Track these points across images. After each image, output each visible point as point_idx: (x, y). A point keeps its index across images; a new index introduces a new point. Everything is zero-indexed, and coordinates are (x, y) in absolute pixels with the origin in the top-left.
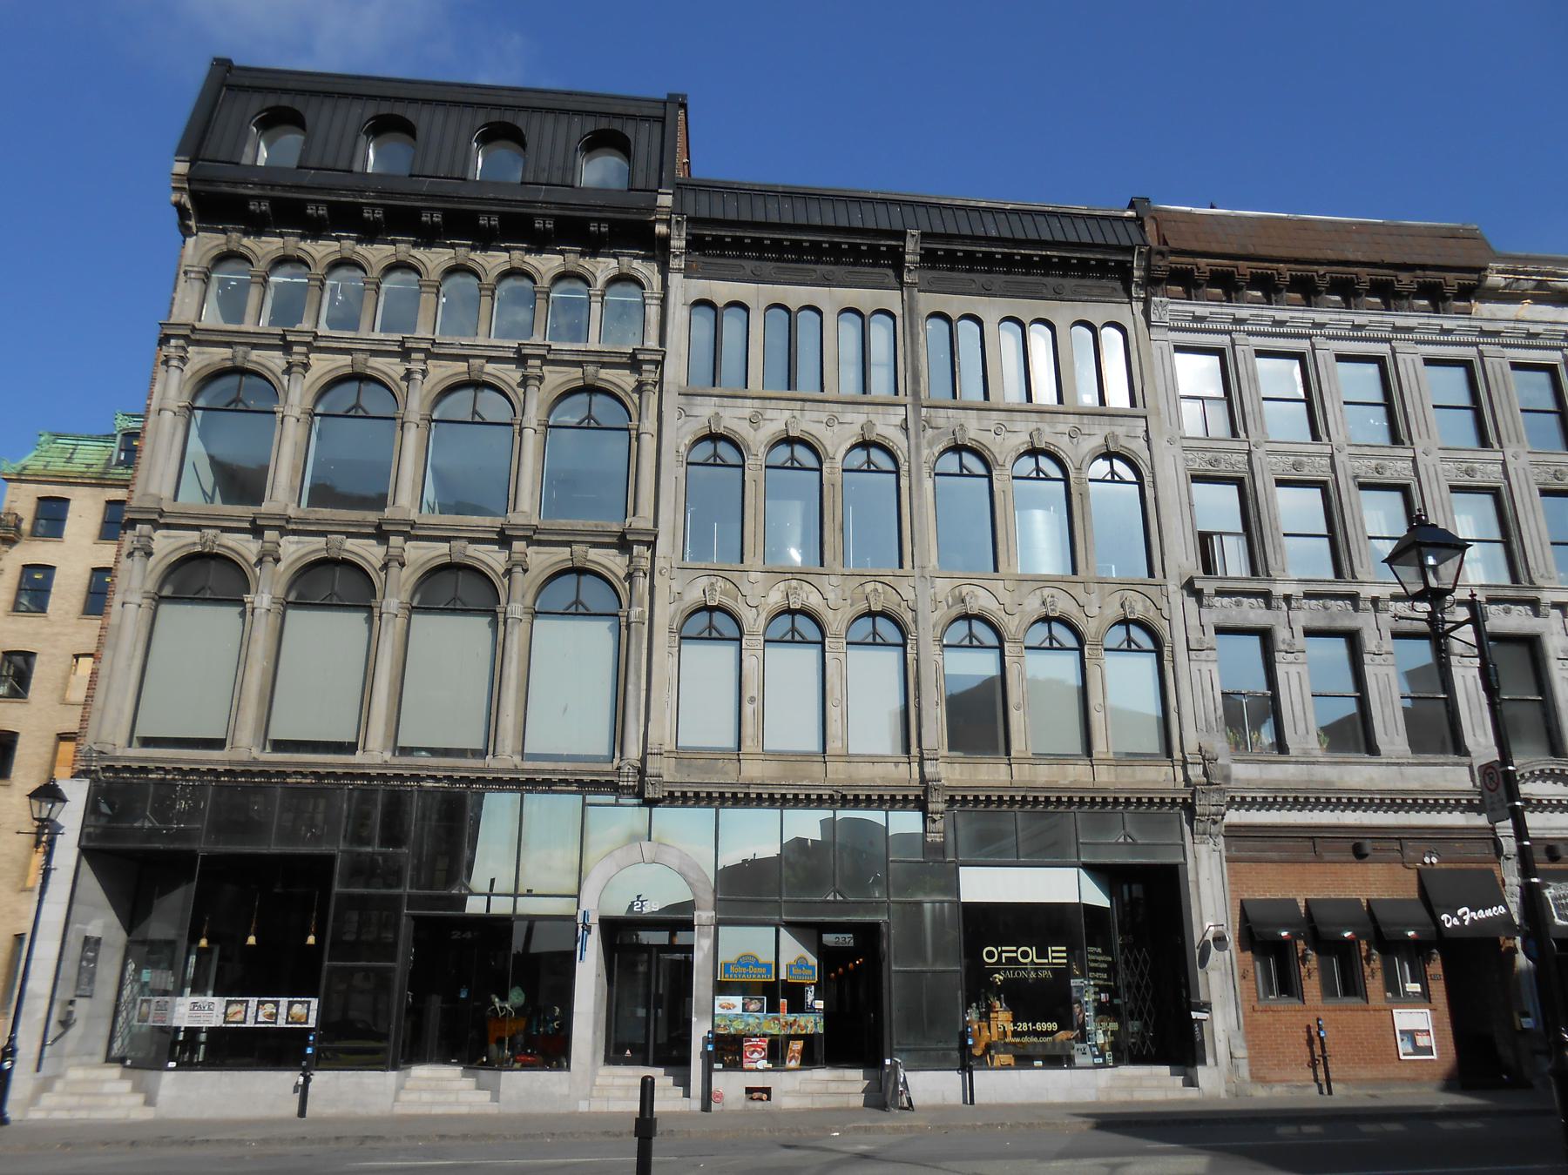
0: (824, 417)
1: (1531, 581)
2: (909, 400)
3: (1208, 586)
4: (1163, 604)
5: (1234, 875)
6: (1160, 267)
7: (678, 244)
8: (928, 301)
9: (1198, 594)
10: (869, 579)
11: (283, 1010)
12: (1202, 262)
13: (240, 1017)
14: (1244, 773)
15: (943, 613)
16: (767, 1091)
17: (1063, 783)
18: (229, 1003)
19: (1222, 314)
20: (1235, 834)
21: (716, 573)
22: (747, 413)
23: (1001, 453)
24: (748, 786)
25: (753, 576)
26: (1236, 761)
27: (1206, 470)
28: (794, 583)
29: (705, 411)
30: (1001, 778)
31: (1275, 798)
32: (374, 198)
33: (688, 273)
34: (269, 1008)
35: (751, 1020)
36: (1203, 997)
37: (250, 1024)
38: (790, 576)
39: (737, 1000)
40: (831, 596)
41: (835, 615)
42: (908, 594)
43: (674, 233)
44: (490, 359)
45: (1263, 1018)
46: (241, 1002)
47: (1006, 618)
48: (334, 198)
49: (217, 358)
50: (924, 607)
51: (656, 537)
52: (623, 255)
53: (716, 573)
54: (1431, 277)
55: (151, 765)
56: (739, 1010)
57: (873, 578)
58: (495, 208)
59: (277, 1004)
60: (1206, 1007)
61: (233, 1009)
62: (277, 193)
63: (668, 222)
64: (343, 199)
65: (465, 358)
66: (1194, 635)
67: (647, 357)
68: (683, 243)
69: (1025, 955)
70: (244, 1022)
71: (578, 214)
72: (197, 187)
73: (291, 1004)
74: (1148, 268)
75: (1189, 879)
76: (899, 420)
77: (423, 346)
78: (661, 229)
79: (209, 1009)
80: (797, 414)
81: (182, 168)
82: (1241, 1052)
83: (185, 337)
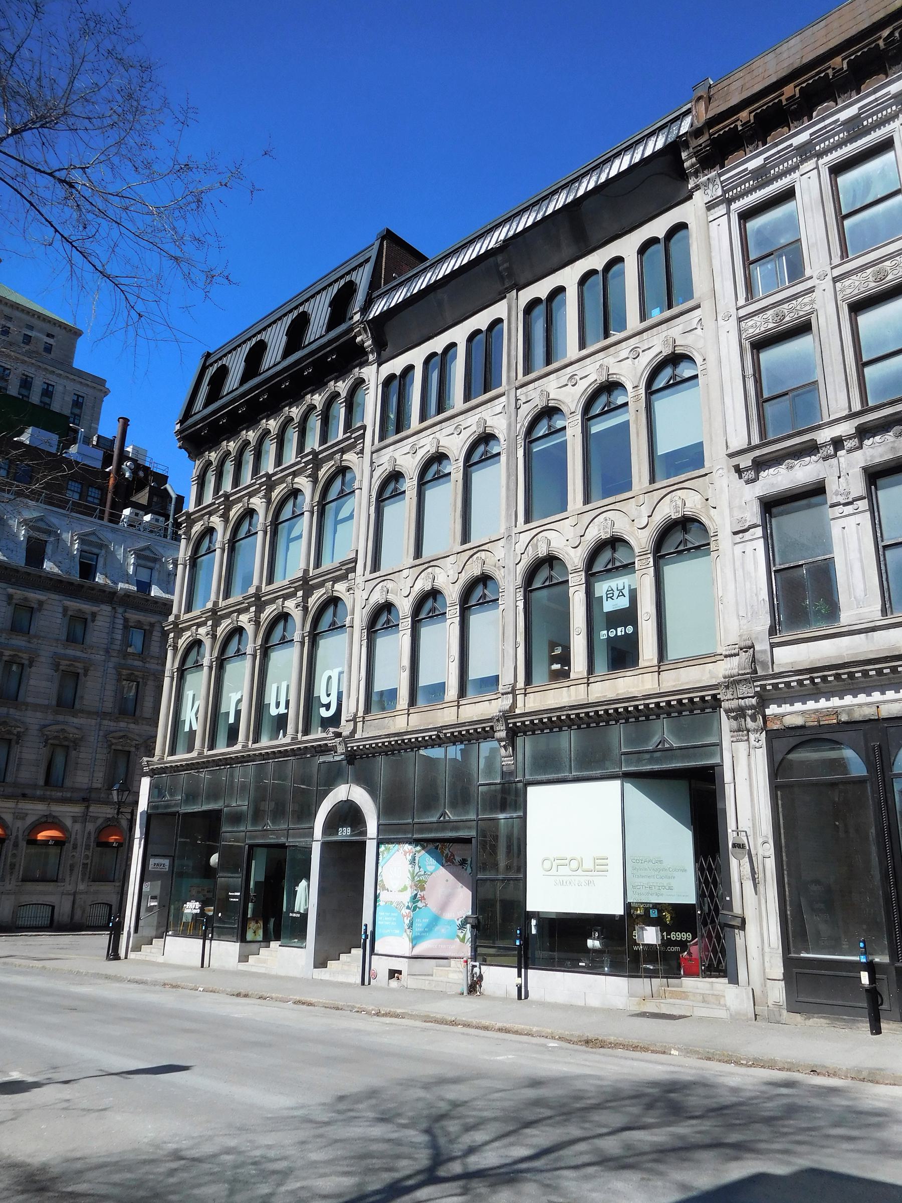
6: (700, 145)
10: (475, 550)
15: (526, 561)
16: (400, 972)
17: (611, 695)
19: (779, 152)
21: (386, 578)
22: (407, 449)
23: (573, 401)
24: (388, 736)
25: (405, 573)
27: (766, 331)
28: (430, 570)
30: (563, 700)
31: (812, 679)
36: (737, 910)
38: (426, 565)
40: (451, 572)
41: (454, 588)
47: (572, 552)
51: (356, 564)
53: (386, 578)
57: (478, 549)
75: (726, 780)
81: (178, 427)
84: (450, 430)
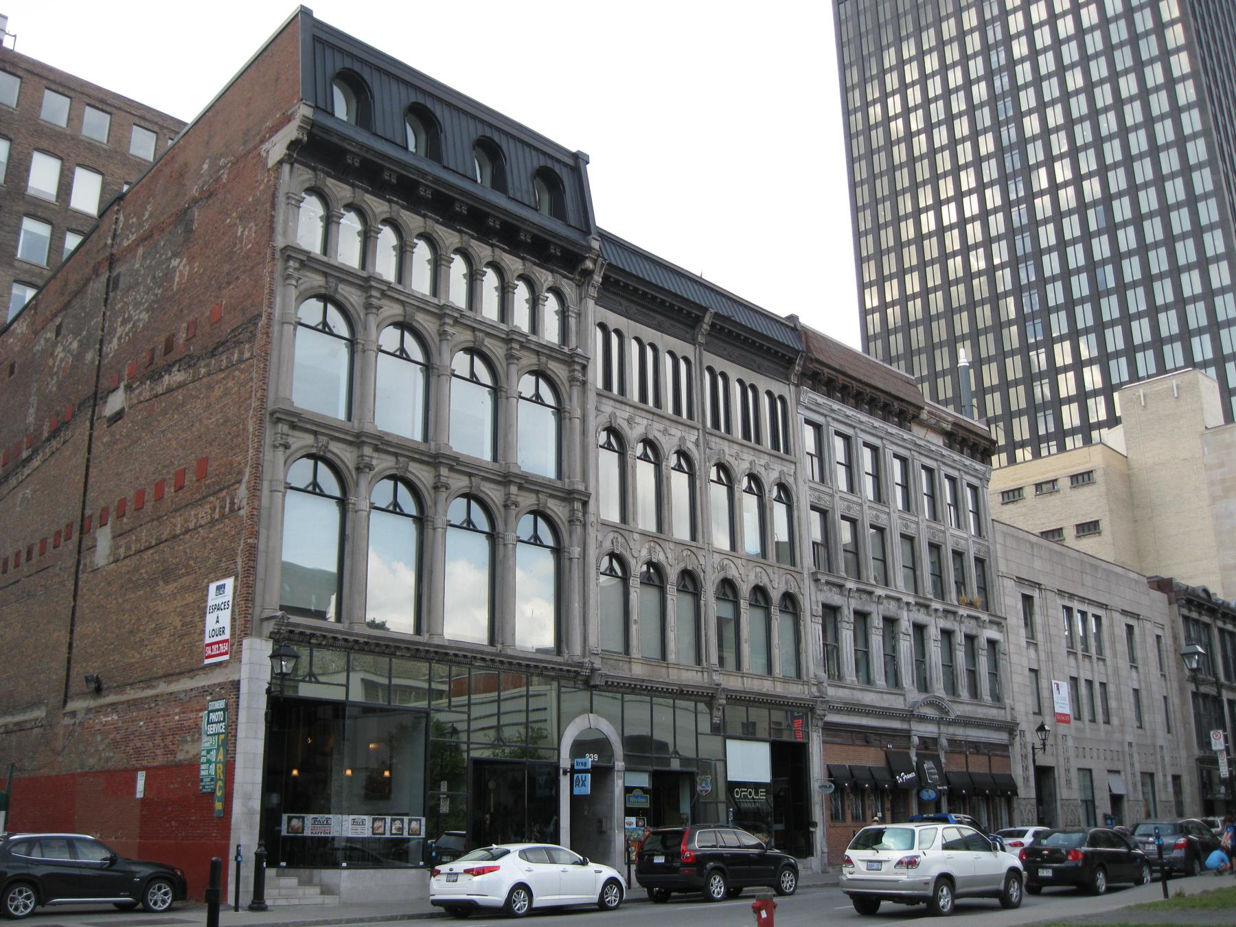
0: (661, 427)
1: (896, 587)
2: (700, 426)
3: (823, 579)
4: (801, 586)
5: (825, 750)
7: (598, 279)
8: (710, 359)
9: (817, 581)
11: (406, 825)
12: (826, 370)
13: (381, 830)
14: (831, 692)
17: (764, 690)
18: (374, 820)
20: (830, 728)
22: (626, 415)
26: (829, 685)
29: (608, 407)
32: (430, 181)
33: (598, 302)
34: (398, 824)
35: (640, 832)
37: (388, 835)
39: (633, 819)
40: (669, 556)
42: (703, 562)
43: (598, 269)
44: (488, 334)
45: (832, 830)
46: (381, 819)
48: (405, 173)
49: (316, 283)
50: (709, 570)
52: (557, 272)
54: (905, 407)
55: (318, 633)
56: (634, 826)
58: (502, 216)
59: (402, 821)
60: (815, 825)
61: (377, 824)
62: (368, 156)
63: (595, 262)
64: (411, 176)
65: (474, 329)
66: (814, 608)
67: (580, 361)
68: (600, 280)
69: (750, 794)
70: (384, 834)
71: (547, 237)
72: (315, 131)
73: (290, 819)
74: (804, 367)
76: (694, 439)
77: (456, 315)
78: (589, 265)
79: (363, 824)
80: (650, 422)
82: (826, 850)
83: (302, 262)
84: (661, 427)
